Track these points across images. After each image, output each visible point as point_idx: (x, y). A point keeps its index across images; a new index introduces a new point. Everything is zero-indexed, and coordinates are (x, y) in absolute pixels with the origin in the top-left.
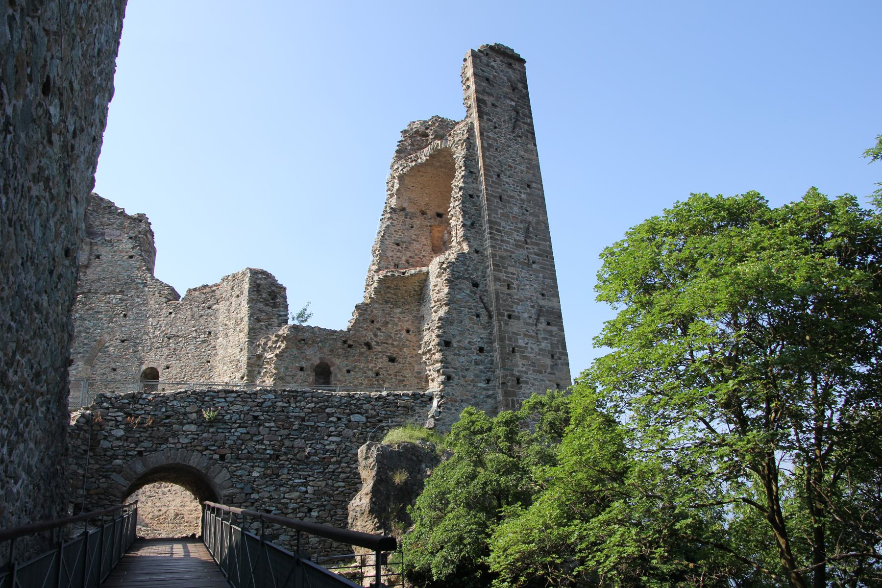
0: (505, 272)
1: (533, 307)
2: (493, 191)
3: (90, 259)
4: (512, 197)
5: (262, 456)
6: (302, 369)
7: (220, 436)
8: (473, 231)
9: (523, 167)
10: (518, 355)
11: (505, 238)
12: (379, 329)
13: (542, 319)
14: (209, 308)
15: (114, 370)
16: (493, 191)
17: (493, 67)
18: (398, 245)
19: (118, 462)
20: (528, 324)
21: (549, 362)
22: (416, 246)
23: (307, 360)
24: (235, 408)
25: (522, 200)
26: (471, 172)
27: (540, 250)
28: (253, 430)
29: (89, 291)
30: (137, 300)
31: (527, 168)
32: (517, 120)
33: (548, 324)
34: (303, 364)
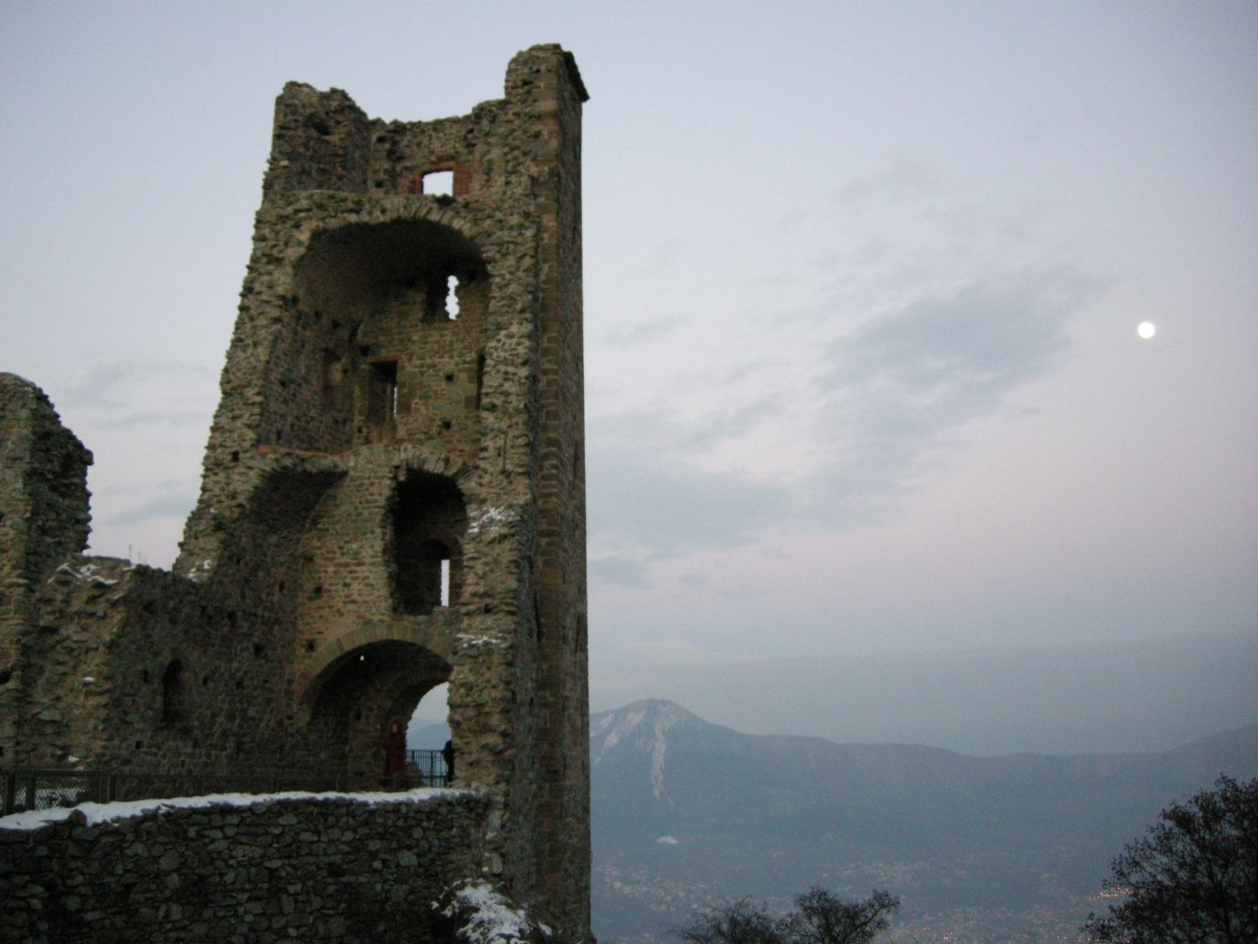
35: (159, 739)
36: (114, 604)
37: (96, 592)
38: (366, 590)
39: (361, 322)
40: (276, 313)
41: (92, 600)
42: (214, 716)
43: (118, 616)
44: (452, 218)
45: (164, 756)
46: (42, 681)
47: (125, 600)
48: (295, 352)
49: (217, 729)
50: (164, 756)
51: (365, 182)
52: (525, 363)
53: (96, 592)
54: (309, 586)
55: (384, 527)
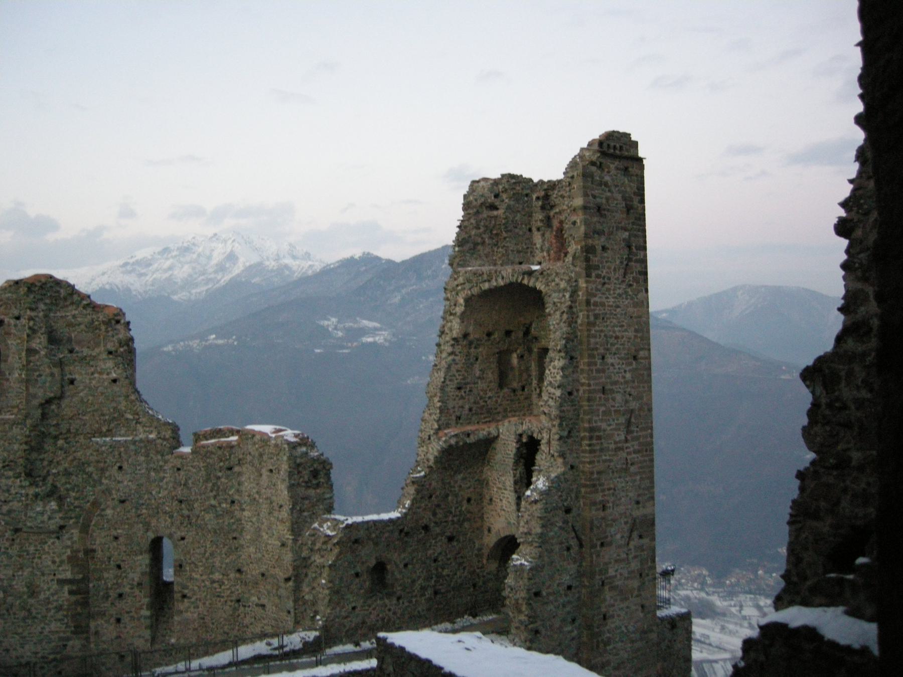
0: (603, 491)
2: (596, 384)
3: (62, 386)
4: (616, 383)
8: (570, 441)
9: (631, 334)
10: (606, 588)
11: (605, 445)
13: (635, 534)
16: (596, 384)
17: (606, 184)
18: (459, 388)
20: (619, 547)
21: (635, 583)
23: (363, 563)
25: (626, 382)
29: (69, 431)
30: (132, 447)
33: (641, 537)
34: (359, 569)
35: (369, 602)
36: (334, 545)
37: (327, 539)
38: (508, 505)
39: (531, 324)
40: (450, 349)
41: (325, 543)
42: (413, 581)
43: (336, 551)
44: (534, 283)
45: (374, 609)
46: (307, 580)
47: (338, 543)
48: (469, 366)
49: (417, 586)
50: (374, 609)
51: (530, 230)
52: (559, 387)
53: (327, 539)
54: (488, 497)
55: (516, 470)
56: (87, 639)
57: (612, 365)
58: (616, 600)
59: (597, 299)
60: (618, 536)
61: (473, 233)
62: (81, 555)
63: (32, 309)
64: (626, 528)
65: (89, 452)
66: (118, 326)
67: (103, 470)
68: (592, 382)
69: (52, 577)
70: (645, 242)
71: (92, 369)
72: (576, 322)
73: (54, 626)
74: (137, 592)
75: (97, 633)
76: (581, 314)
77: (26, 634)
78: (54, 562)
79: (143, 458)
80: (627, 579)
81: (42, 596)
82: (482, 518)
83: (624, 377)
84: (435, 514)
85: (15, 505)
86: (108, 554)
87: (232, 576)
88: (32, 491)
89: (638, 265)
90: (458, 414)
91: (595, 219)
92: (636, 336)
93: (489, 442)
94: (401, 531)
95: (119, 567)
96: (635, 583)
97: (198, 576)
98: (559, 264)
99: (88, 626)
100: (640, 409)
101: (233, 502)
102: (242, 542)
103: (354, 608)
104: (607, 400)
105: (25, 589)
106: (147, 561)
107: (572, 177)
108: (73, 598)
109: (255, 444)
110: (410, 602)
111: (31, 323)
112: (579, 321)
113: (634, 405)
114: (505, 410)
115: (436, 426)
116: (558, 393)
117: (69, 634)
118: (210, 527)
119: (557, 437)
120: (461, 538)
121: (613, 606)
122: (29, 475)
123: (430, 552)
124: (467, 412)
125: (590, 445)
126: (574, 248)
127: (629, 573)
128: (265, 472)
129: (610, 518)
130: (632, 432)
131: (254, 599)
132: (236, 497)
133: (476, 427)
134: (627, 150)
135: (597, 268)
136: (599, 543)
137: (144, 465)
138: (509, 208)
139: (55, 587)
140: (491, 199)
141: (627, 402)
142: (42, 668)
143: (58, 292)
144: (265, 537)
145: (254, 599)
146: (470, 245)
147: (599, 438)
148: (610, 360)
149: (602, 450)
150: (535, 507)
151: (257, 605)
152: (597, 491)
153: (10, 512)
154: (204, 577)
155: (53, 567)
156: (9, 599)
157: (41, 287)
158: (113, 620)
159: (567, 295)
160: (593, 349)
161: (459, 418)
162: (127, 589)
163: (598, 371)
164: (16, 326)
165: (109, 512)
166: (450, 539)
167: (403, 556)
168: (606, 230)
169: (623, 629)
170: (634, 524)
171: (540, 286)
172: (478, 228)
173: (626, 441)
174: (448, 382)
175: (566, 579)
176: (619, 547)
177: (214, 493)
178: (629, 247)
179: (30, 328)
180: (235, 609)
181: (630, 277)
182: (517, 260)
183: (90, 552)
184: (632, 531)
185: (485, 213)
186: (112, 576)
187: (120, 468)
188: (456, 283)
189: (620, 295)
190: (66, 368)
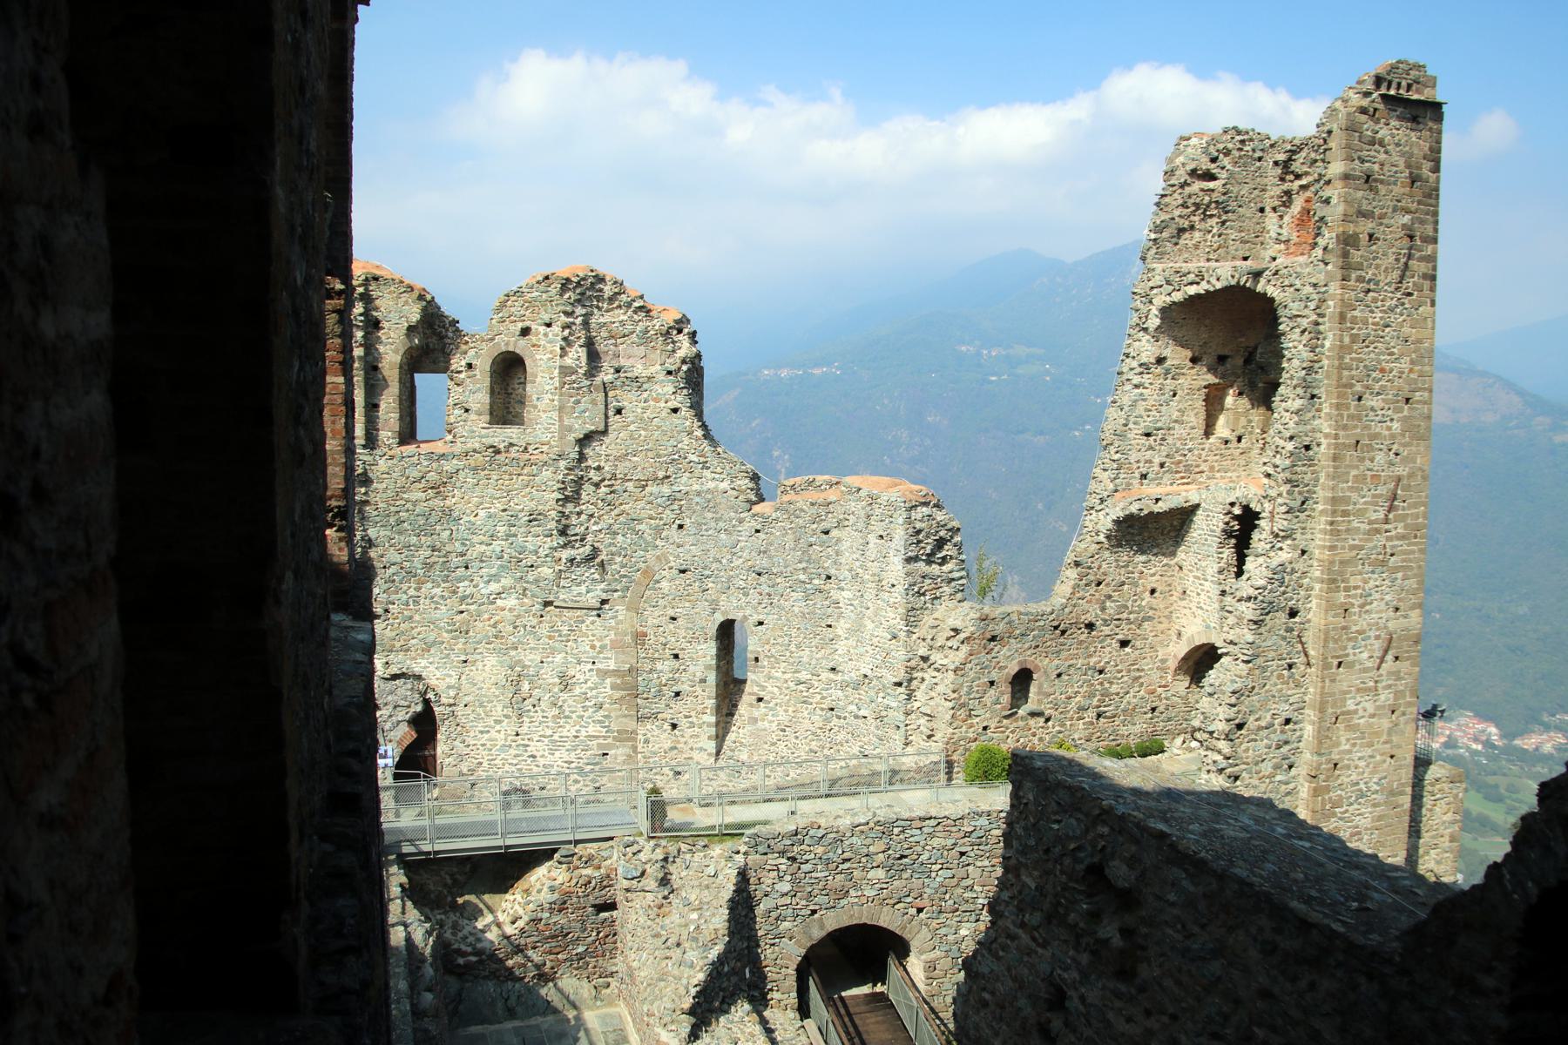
0: (1347, 589)
1: (1377, 638)
2: (1347, 437)
3: (607, 417)
4: (1375, 436)
5: (972, 907)
6: (992, 683)
7: (916, 883)
8: (1302, 516)
9: (1404, 364)
11: (1355, 524)
12: (1109, 597)
13: (1389, 657)
14: (827, 533)
15: (674, 619)
18: (1148, 435)
19: (786, 924)
20: (1366, 670)
22: (1179, 431)
24: (936, 842)
25: (1393, 436)
26: (1313, 397)
27: (1406, 527)
28: (961, 873)
30: (697, 499)
31: (1412, 362)
32: (1410, 257)
34: (994, 676)
39: (1256, 348)
43: (965, 649)
46: (923, 687)
51: (1262, 210)
54: (1180, 589)
56: (635, 748)
57: (1372, 409)
58: (1354, 745)
59: (1356, 313)
60: (1365, 655)
61: (1177, 213)
62: (628, 639)
63: (567, 314)
64: (1377, 646)
65: (641, 504)
66: (680, 337)
67: (658, 531)
68: (1341, 433)
69: (590, 666)
70: (1436, 230)
71: (645, 395)
72: (1323, 346)
73: (593, 729)
74: (698, 689)
75: (647, 741)
76: (1330, 335)
77: (556, 737)
78: (593, 647)
79: (710, 515)
80: (1372, 716)
81: (577, 691)
82: (1169, 617)
83: (1389, 428)
84: (1103, 609)
85: (546, 571)
86: (662, 640)
87: (826, 675)
88: (565, 554)
89: (1423, 264)
90: (1144, 471)
91: (1360, 194)
92: (1411, 371)
93: (1183, 517)
94: (1056, 628)
95: (676, 656)
96: (1385, 723)
97: (779, 675)
98: (1301, 259)
99: (634, 732)
100: (1411, 476)
101: (829, 577)
102: (840, 632)
103: (985, 728)
104: (1362, 460)
105: (557, 680)
106: (714, 651)
107: (1330, 132)
108: (618, 694)
109: (859, 499)
110: (1063, 725)
111: (567, 332)
112: (1327, 344)
113: (1401, 470)
114: (1212, 468)
115: (1111, 486)
116: (1290, 446)
117: (610, 740)
118: (796, 609)
119: (1284, 509)
120: (1138, 644)
121: (1350, 752)
122: (563, 532)
123: (1093, 661)
124: (1157, 468)
125: (1332, 523)
126: (1328, 238)
127: (1378, 708)
128: (872, 539)
129: (1354, 628)
130: (1397, 508)
131: (853, 708)
132: (832, 572)
133: (1169, 489)
134: (1418, 91)
135: (1359, 267)
136: (1335, 663)
137: (713, 524)
138: (1231, 175)
139: (595, 679)
140: (1205, 164)
141: (1391, 464)
142: (576, 781)
143: (601, 290)
144: (870, 625)
145: (853, 708)
146: (1172, 230)
147: (1345, 513)
148: (1371, 401)
149: (1348, 530)
150: (1243, 606)
151: (856, 717)
152: (1337, 589)
153: (537, 581)
154: (787, 676)
155: (592, 653)
156: (536, 692)
157: (578, 284)
158: (667, 726)
159: (1312, 305)
160: (1345, 386)
161: (1144, 476)
162: (684, 688)
163: (1351, 417)
164: (546, 335)
165: (664, 584)
166: (1124, 644)
167: (1056, 662)
168: (1377, 212)
169: (1362, 786)
170: (1390, 640)
171: (1271, 291)
172: (1184, 205)
173: (1386, 521)
174: (1131, 426)
175: (1285, 710)
176: (1366, 670)
177: (804, 565)
178: (1411, 237)
179: (565, 339)
180: (827, 720)
181: (1409, 284)
182: (1241, 253)
183: (640, 637)
184: (1386, 652)
185: (1198, 185)
186: (666, 668)
187: (681, 527)
188: (1151, 284)
189: (1392, 310)
190: (611, 394)
